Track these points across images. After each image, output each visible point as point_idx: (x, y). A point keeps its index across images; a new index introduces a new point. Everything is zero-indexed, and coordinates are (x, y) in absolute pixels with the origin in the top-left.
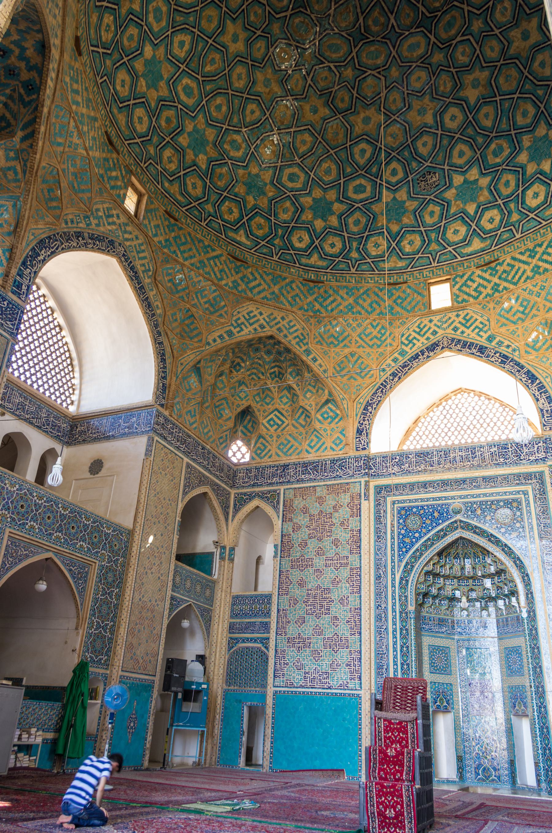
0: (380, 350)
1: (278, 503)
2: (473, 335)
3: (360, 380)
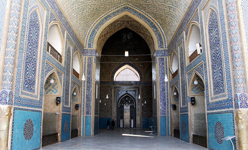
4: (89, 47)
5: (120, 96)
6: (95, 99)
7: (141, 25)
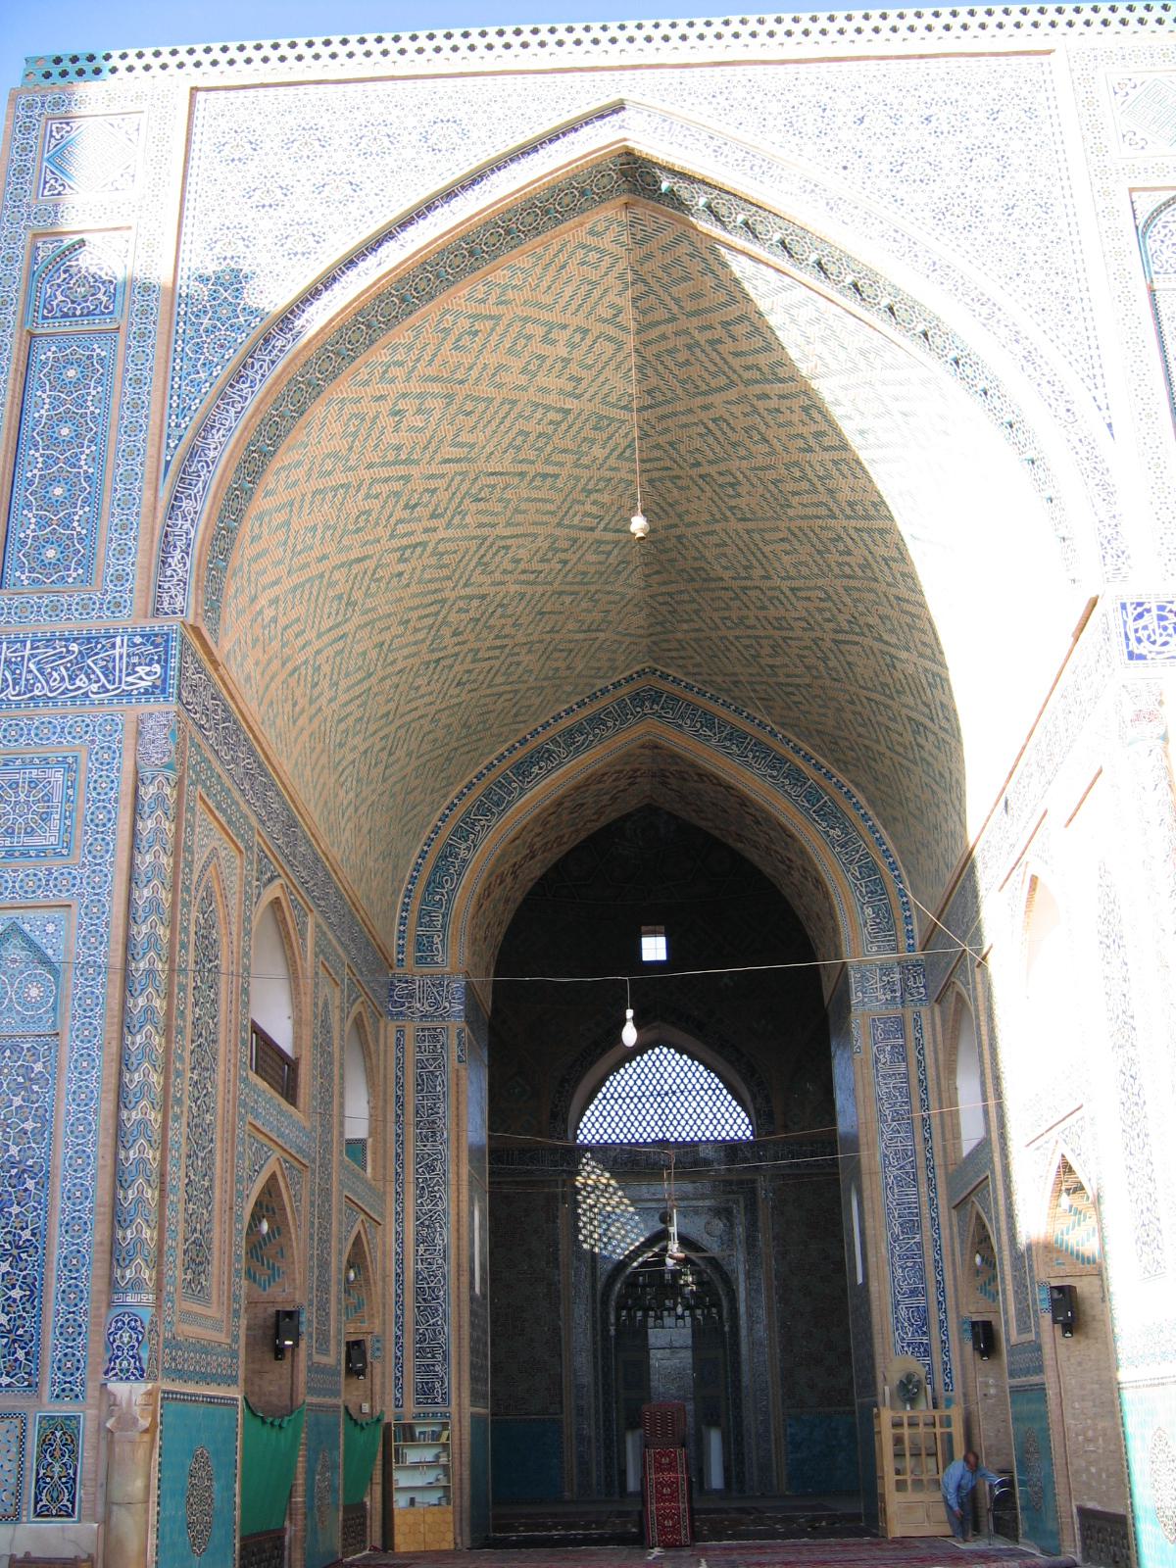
4: (420, 960)
6: (473, 1299)
7: (744, 801)
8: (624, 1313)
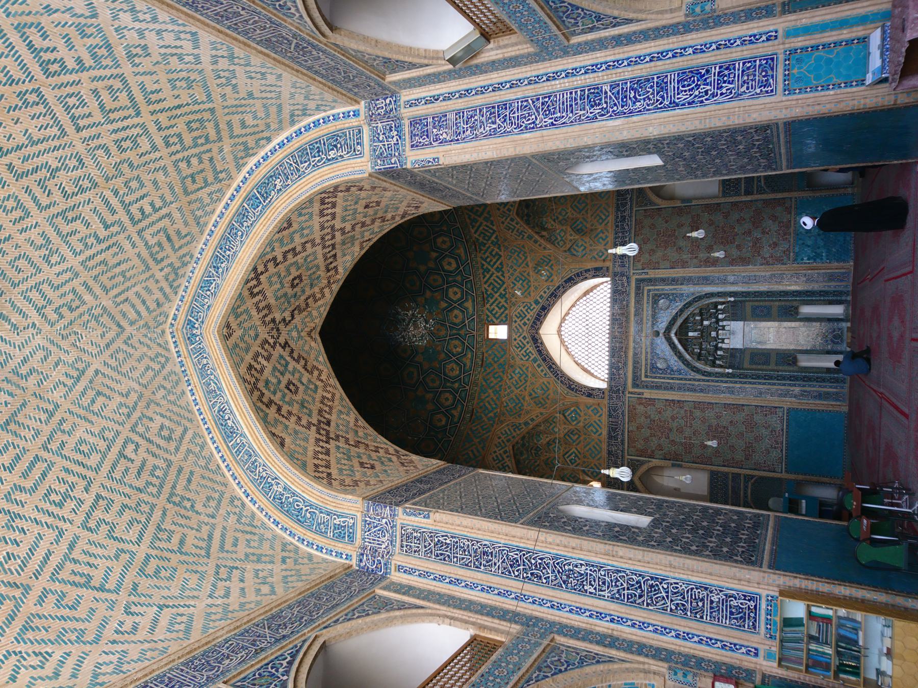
0: (530, 375)
1: (638, 461)
2: (532, 313)
3: (551, 391)
5: (674, 362)
8: (718, 362)
